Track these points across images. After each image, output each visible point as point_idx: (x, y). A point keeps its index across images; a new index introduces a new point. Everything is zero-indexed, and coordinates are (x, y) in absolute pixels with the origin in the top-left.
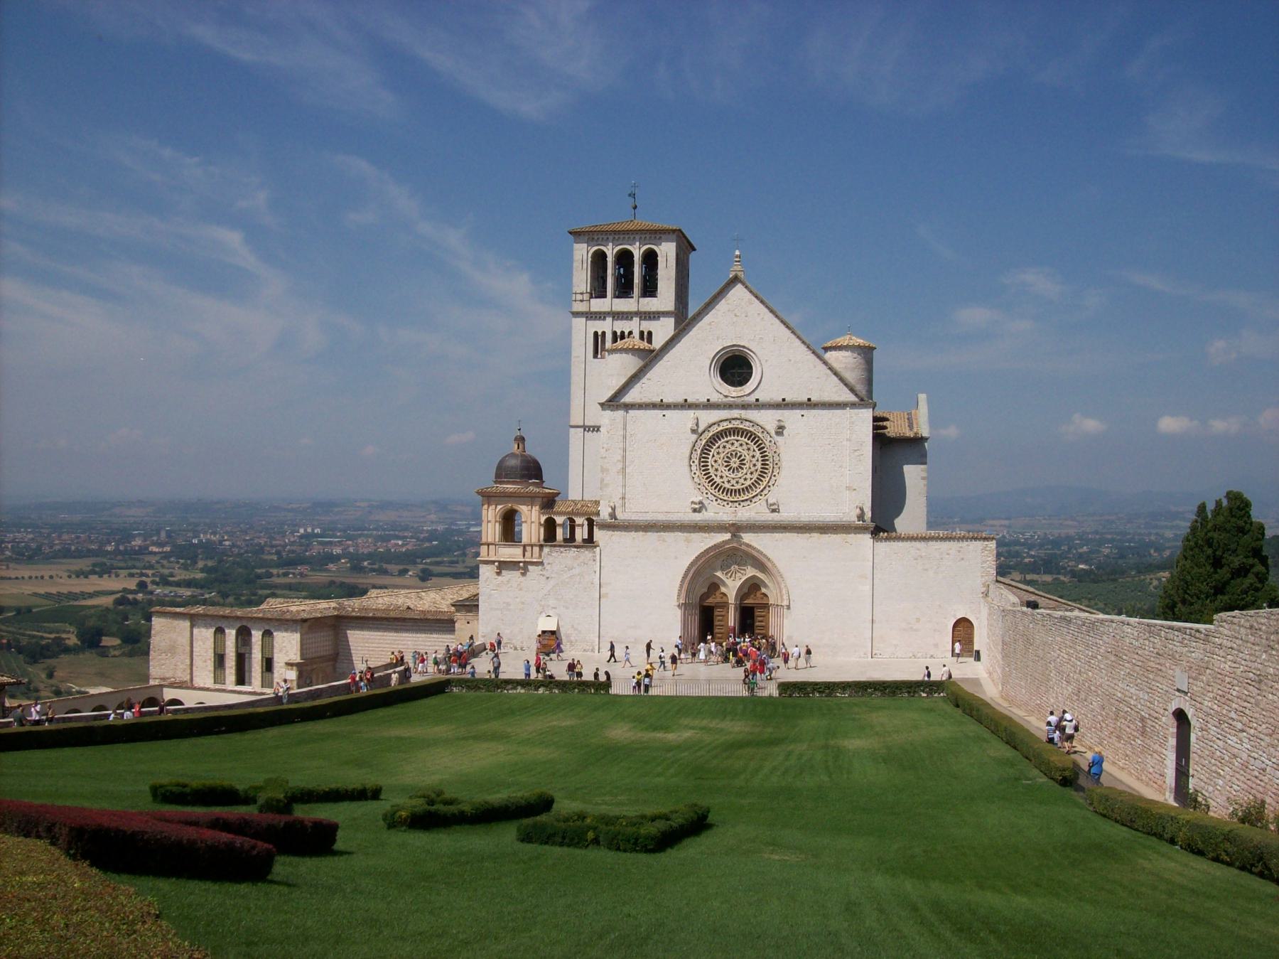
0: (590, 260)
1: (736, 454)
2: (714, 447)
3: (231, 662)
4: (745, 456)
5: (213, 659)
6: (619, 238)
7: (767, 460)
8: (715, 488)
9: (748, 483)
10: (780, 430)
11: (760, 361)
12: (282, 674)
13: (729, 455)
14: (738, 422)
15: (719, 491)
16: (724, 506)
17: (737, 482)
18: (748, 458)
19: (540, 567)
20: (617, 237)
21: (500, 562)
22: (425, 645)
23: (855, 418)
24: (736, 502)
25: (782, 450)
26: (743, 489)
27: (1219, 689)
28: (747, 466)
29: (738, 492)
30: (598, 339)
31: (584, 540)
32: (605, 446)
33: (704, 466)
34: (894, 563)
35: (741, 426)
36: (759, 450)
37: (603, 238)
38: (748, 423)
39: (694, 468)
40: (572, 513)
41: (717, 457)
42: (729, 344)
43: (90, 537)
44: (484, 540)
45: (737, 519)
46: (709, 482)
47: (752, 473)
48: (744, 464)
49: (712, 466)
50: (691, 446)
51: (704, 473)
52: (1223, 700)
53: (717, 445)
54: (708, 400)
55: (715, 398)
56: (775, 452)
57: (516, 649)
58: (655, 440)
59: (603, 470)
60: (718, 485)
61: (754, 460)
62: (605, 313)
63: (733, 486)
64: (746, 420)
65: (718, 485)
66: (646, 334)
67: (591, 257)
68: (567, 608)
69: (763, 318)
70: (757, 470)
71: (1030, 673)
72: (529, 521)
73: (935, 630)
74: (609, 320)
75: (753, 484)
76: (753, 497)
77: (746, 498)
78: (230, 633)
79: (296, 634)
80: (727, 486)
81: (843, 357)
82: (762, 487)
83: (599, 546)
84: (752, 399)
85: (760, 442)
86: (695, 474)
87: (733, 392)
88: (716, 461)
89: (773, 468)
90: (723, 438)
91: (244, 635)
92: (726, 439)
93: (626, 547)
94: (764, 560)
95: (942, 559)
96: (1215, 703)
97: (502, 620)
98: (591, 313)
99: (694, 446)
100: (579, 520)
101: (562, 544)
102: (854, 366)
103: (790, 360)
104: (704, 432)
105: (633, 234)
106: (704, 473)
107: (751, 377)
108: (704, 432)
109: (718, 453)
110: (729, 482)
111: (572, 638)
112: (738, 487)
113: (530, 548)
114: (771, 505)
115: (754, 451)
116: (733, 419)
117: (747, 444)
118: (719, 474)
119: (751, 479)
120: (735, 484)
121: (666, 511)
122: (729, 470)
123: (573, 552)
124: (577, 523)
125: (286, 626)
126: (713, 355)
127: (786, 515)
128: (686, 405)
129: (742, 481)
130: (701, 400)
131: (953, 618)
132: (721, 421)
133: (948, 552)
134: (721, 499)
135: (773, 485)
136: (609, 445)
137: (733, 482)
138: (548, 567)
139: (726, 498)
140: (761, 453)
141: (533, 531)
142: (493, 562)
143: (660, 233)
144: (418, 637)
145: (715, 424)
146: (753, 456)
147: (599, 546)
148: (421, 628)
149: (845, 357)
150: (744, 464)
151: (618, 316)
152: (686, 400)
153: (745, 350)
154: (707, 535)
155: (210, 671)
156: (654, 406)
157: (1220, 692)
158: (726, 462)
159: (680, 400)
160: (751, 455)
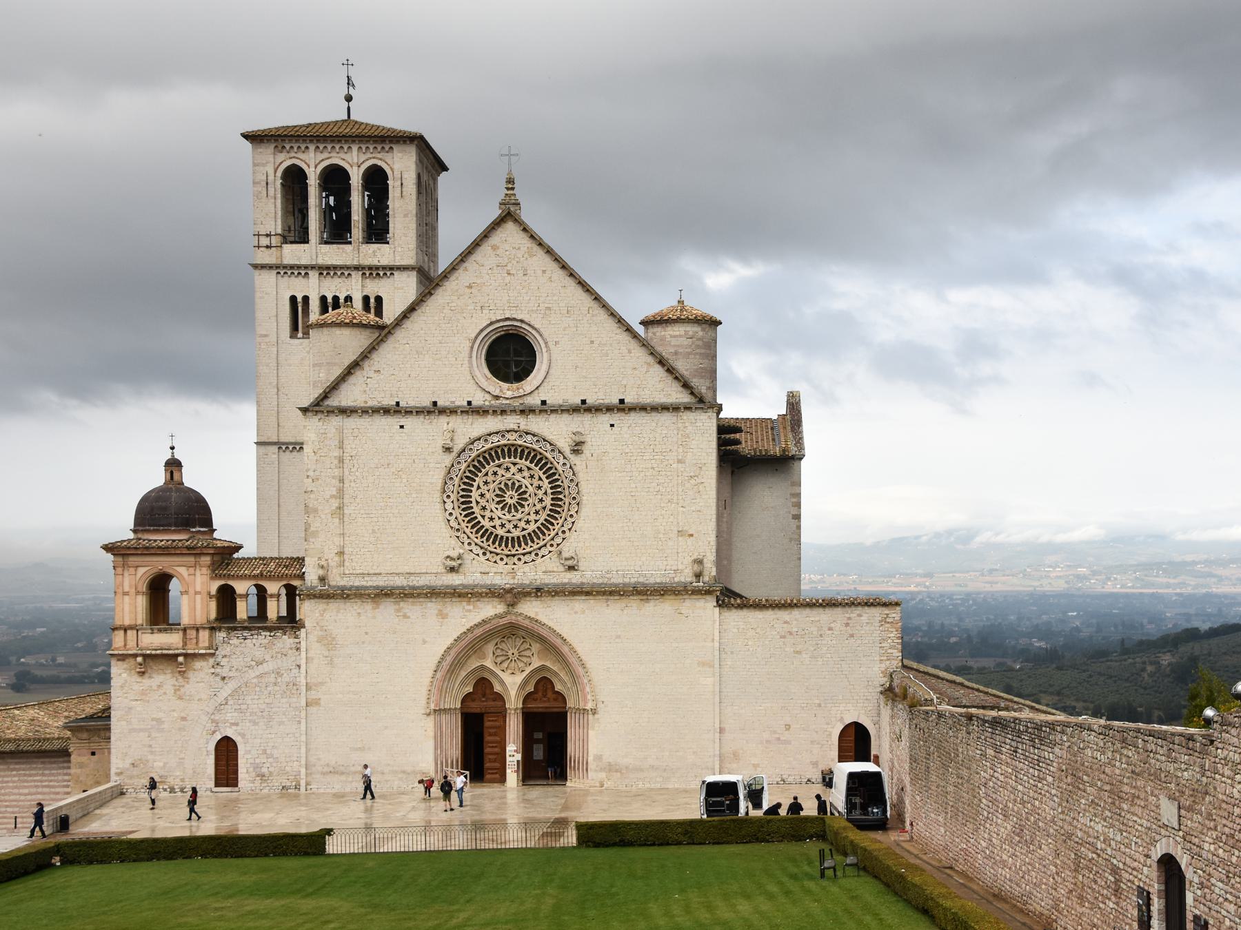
0: (279, 181)
1: (513, 484)
2: (480, 474)
4: (526, 487)
6: (325, 147)
7: (560, 493)
8: (482, 536)
9: (532, 527)
10: (577, 448)
11: (546, 343)
13: (502, 486)
14: (515, 436)
15: (488, 540)
16: (495, 562)
17: (516, 527)
18: (531, 489)
19: (211, 661)
20: (321, 147)
21: (145, 656)
22: (20, 794)
23: (690, 428)
24: (514, 556)
25: (581, 477)
26: (524, 536)
27: (1224, 826)
28: (530, 501)
29: (517, 541)
30: (297, 307)
31: (280, 618)
32: (311, 473)
33: (466, 504)
34: (750, 643)
35: (520, 442)
36: (547, 478)
37: (299, 147)
38: (529, 437)
39: (449, 506)
40: (261, 576)
41: (484, 489)
42: (499, 318)
43: (54, 660)
44: (118, 622)
45: (516, 582)
46: (473, 527)
47: (537, 513)
48: (526, 500)
49: (478, 503)
50: (443, 473)
51: (464, 513)
52: (1231, 842)
53: (483, 470)
54: (469, 403)
55: (479, 399)
56: (572, 480)
57: (172, 790)
58: (388, 465)
59: (308, 510)
60: (487, 530)
61: (540, 493)
62: (306, 267)
63: (509, 532)
64: (527, 433)
65: (487, 530)
66: (372, 300)
67: (282, 178)
68: (255, 723)
69: (550, 278)
70: (544, 508)
71: (951, 803)
72: (191, 591)
73: (812, 742)
74: (314, 275)
75: (538, 528)
76: (540, 549)
77: (528, 549)
80: (500, 532)
81: (671, 336)
82: (553, 533)
83: (304, 627)
84: (535, 401)
85: (549, 465)
86: (451, 514)
87: (507, 390)
88: (482, 495)
89: (570, 504)
90: (494, 461)
92: (497, 462)
93: (348, 627)
94: (558, 642)
95: (821, 636)
96: (1220, 847)
97: (150, 746)
98: (285, 267)
99: (449, 473)
100: (272, 587)
101: (246, 624)
102: (689, 350)
103: (592, 342)
104: (464, 451)
105: (346, 142)
106: (464, 513)
107: (533, 367)
108: (464, 450)
109: (486, 483)
110: (503, 526)
111: (264, 770)
112: (516, 533)
113: (194, 632)
114: (566, 559)
115: (540, 479)
116: (508, 431)
117: (529, 469)
118: (488, 514)
119: (536, 521)
120: (513, 530)
121: (408, 571)
122: (503, 509)
123: (263, 638)
124: (269, 592)
126: (478, 331)
127: (588, 574)
128: (435, 409)
129: (522, 524)
130: (458, 403)
131: (839, 723)
132: (490, 435)
133: (832, 625)
134: (491, 552)
135: (570, 529)
136: (317, 473)
137: (509, 526)
138: (224, 662)
139: (498, 551)
140: (550, 483)
141: (199, 606)
142: (135, 656)
143: (391, 142)
144: (8, 782)
145: (479, 439)
146: (539, 487)
147: (304, 627)
148: (12, 767)
149: (675, 336)
150: (526, 500)
151: (326, 270)
152: (435, 403)
153: (524, 326)
154: (471, 607)
156: (386, 411)
157: (1227, 830)
158: (497, 496)
159: (426, 403)
160: (536, 483)
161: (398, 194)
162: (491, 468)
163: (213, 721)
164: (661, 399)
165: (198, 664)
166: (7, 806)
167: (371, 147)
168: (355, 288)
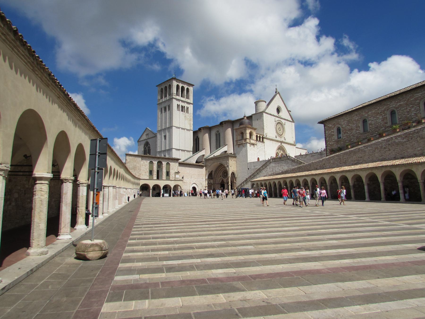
3: (155, 173)
5: (149, 172)
9: (282, 134)
12: (173, 176)
20: (182, 83)
30: (178, 106)
55: (277, 115)
78: (155, 163)
79: (177, 164)
84: (281, 117)
91: (160, 164)
94: (285, 149)
112: (280, 134)
125: (174, 162)
151: (182, 101)
155: (147, 176)
159: (273, 114)
161: (191, 93)
162: (278, 125)
163: (257, 155)
164: (290, 120)
165: (255, 146)
166: (190, 174)
167: (188, 85)
168: (186, 105)
